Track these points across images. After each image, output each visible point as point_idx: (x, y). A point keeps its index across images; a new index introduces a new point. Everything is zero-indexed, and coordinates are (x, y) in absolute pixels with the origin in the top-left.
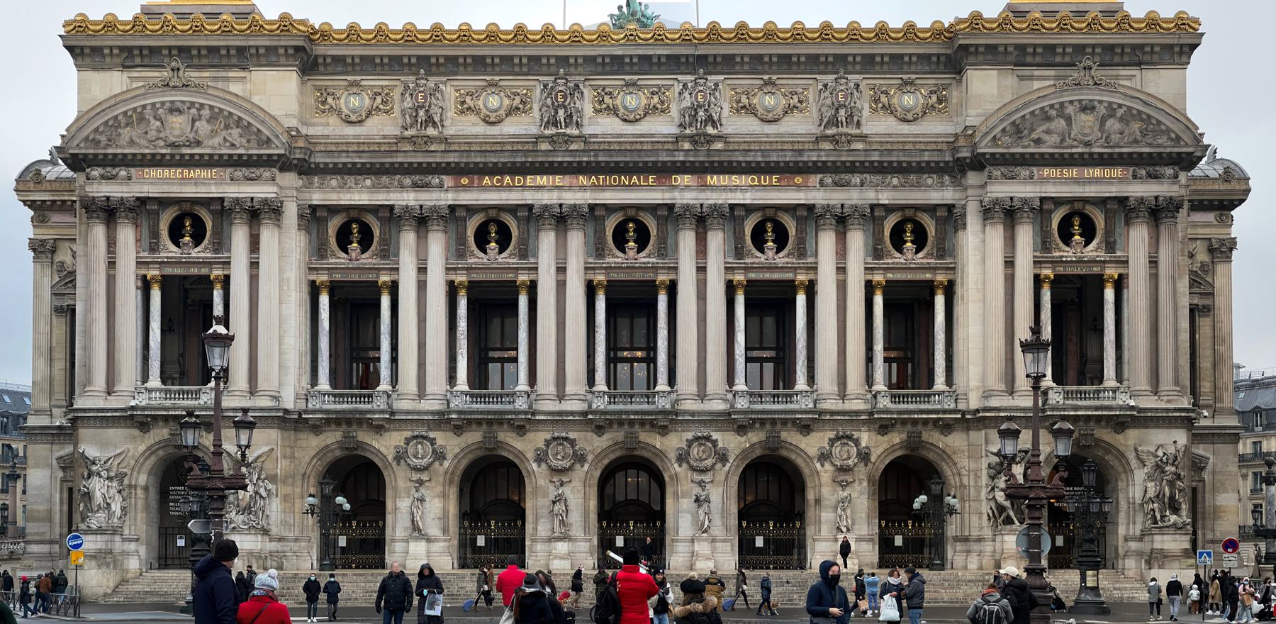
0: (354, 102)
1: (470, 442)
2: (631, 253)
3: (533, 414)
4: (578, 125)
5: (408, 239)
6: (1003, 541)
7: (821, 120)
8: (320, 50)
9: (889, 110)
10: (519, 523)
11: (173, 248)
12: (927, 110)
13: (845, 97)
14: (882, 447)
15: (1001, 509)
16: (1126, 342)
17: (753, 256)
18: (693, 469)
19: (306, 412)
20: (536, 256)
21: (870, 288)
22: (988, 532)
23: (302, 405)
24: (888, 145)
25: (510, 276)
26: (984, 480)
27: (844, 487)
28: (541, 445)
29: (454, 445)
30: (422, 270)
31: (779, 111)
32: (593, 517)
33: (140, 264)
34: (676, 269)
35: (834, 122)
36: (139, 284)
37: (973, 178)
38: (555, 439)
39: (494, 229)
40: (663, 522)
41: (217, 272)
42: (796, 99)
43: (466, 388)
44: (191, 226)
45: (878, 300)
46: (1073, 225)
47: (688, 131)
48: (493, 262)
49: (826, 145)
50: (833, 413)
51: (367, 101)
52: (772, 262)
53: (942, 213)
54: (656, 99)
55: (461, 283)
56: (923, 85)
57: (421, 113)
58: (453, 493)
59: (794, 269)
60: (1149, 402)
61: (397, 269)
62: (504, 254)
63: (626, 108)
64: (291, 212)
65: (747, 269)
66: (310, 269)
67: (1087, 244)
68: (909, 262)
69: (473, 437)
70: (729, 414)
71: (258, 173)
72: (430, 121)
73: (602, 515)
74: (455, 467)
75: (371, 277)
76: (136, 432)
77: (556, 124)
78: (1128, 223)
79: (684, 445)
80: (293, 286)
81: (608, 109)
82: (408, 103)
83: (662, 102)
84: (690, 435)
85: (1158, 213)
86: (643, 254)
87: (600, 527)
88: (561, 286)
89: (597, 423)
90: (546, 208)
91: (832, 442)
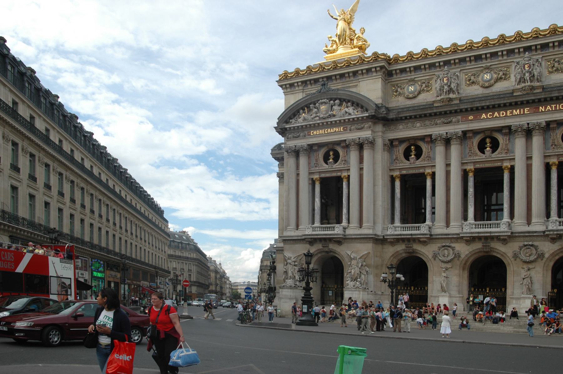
5: (440, 150)
10: (503, 290)
20: (513, 152)
25: (499, 164)
29: (464, 250)
36: (310, 182)
39: (489, 140)
43: (473, 222)
48: (488, 159)
57: (446, 87)
58: (466, 275)
61: (435, 166)
64: (379, 142)
69: (478, 246)
71: (362, 126)
72: (450, 91)
75: (421, 171)
80: (380, 177)
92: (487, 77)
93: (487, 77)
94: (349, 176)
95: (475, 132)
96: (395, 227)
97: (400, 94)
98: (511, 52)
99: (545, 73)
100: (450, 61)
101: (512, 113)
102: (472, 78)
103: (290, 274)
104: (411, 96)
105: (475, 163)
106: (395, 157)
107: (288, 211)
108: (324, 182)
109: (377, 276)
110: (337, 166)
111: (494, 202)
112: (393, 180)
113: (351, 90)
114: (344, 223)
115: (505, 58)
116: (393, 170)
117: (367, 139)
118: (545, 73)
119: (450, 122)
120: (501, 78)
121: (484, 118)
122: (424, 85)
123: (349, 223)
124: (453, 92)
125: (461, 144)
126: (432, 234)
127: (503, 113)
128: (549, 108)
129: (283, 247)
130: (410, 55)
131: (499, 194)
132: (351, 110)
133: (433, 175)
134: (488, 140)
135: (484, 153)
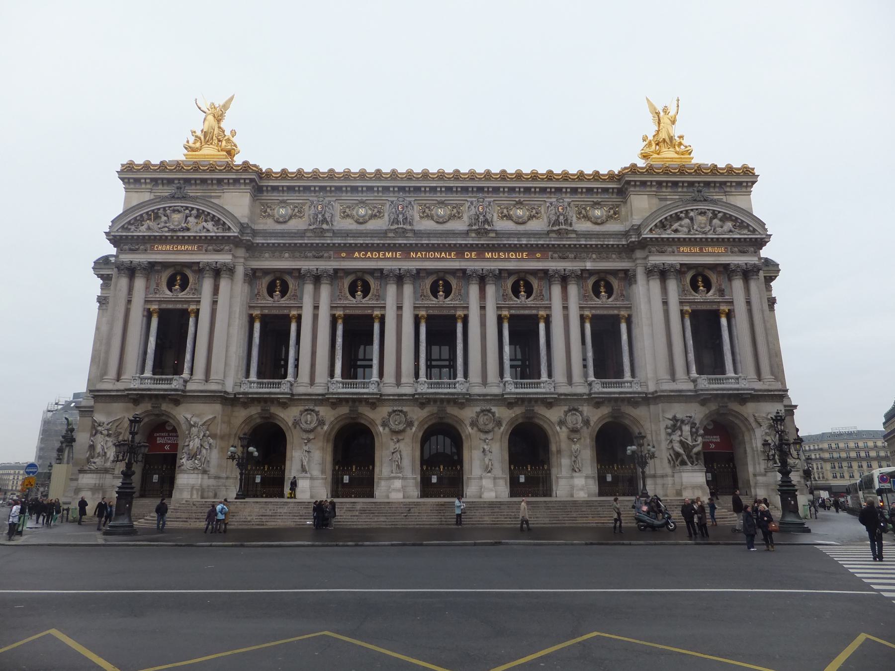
0: (282, 211)
1: (341, 413)
2: (441, 298)
3: (381, 395)
4: (411, 224)
5: (309, 288)
6: (681, 477)
7: (550, 223)
8: (265, 183)
9: (587, 218)
11: (168, 292)
12: (609, 218)
13: (563, 209)
14: (596, 416)
15: (678, 455)
16: (737, 350)
17: (512, 300)
18: (480, 430)
19: (239, 394)
20: (384, 299)
21: (582, 319)
22: (669, 471)
23: (238, 390)
24: (588, 235)
26: (663, 436)
27: (575, 443)
28: (385, 415)
30: (316, 308)
31: (526, 218)
32: (418, 463)
33: (147, 302)
34: (467, 307)
35: (557, 222)
36: (145, 313)
37: (639, 254)
38: (394, 411)
40: (462, 467)
41: (193, 307)
42: (534, 211)
43: (340, 379)
44: (181, 280)
45: (588, 326)
46: (698, 281)
47: (474, 227)
48: (359, 303)
49: (553, 235)
50: (565, 395)
51: (290, 211)
52: (524, 303)
53: (621, 275)
54: (455, 211)
55: (339, 316)
56: (605, 205)
57: (320, 216)
59: (537, 308)
60: (758, 386)
62: (367, 298)
63: (438, 215)
65: (510, 308)
66: (250, 307)
67: (708, 291)
68: (604, 304)
70: (503, 395)
72: (324, 221)
73: (423, 462)
74: (332, 429)
75: (286, 312)
76: (131, 405)
77: (397, 223)
78: (730, 280)
79: (474, 415)
80: (237, 315)
81: (427, 216)
82: (312, 211)
83: (459, 213)
84: (478, 409)
85: (747, 274)
86: (448, 299)
87: (422, 469)
88: (399, 318)
89: (421, 401)
90: (391, 271)
91: (566, 413)
92: (362, 211)
93: (362, 211)
94: (198, 310)
95: (347, 272)
96: (251, 383)
97: (269, 216)
98: (386, 189)
99: (417, 217)
100: (326, 187)
101: (384, 255)
102: (347, 210)
103: (99, 449)
104: (281, 220)
105: (345, 308)
106: (256, 292)
107: (107, 352)
108: (164, 315)
109: (222, 450)
110: (182, 295)
111: (361, 356)
112: (251, 320)
113: (213, 200)
114: (186, 374)
115: (380, 194)
116: (254, 307)
117: (225, 264)
118: (417, 217)
119: (322, 257)
120: (375, 216)
121: (356, 258)
122: (296, 210)
123: (192, 374)
124: (327, 223)
125: (331, 284)
126: (294, 392)
127: (375, 255)
128: (419, 254)
129: (92, 407)
130: (284, 174)
131: (367, 347)
132: (210, 225)
133: (299, 318)
134: (359, 283)
135: (354, 297)
